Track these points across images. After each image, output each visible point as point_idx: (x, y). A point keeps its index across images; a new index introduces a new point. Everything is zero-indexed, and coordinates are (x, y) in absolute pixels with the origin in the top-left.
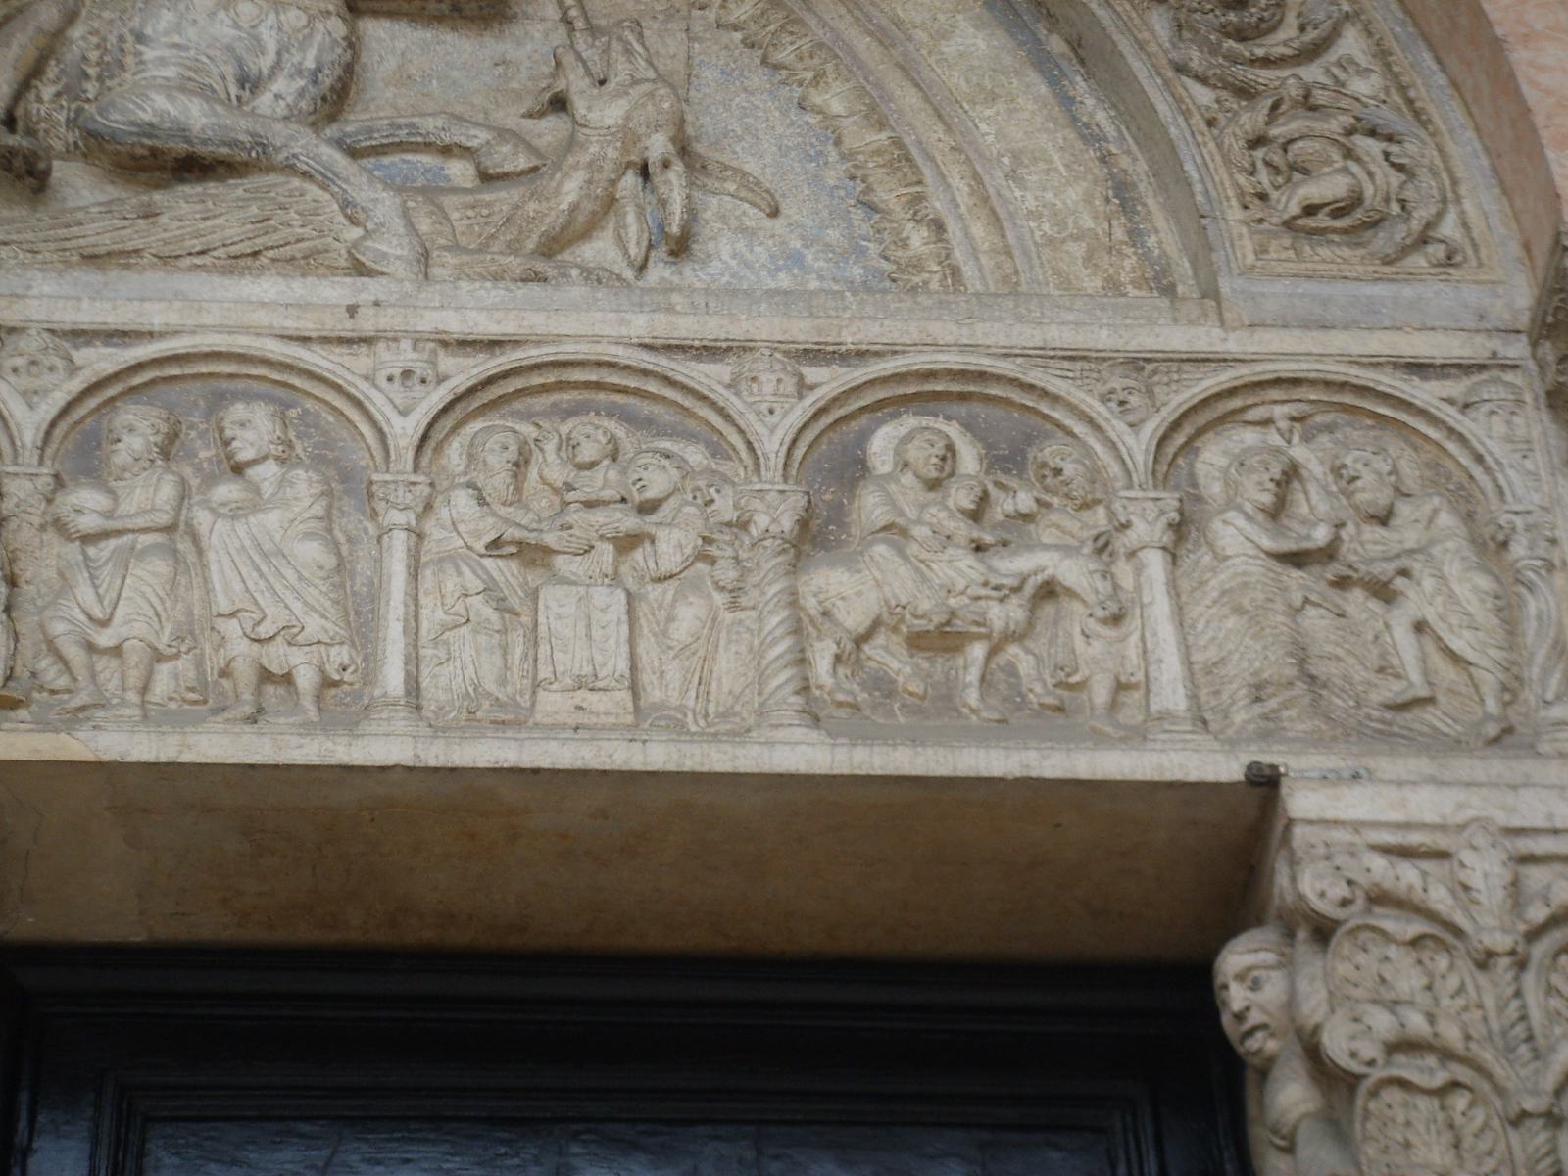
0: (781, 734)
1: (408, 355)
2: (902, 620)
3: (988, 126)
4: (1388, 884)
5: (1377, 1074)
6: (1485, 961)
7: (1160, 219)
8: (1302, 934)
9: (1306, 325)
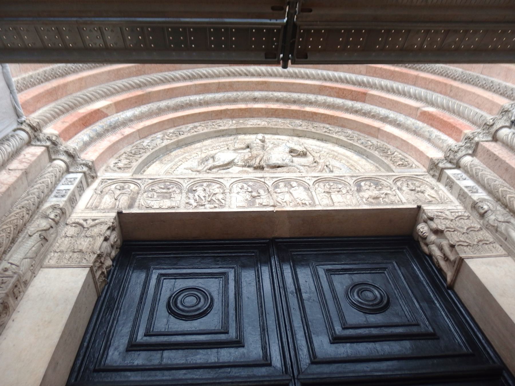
1: (309, 178)
3: (360, 163)
6: (452, 220)
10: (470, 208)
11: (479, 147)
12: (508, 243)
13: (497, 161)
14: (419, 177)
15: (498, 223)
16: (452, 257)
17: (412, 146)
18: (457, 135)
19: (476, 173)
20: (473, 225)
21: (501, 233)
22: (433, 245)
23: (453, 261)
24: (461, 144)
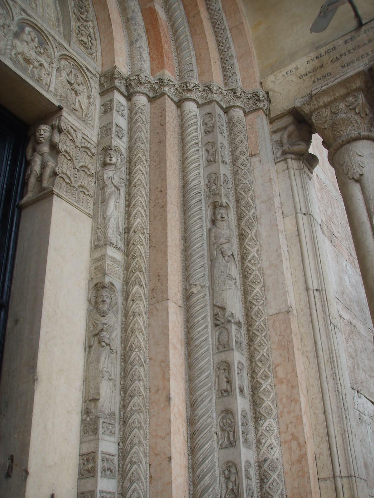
0: (7, 59)
2: (24, 55)
4: (70, 130)
5: (63, 153)
6: (76, 147)
7: (61, 27)
8: (56, 130)
9: (78, 54)
10: (102, 148)
11: (162, 99)
12: (101, 207)
13: (161, 127)
14: (88, 73)
15: (111, 183)
16: (45, 184)
17: (112, 33)
18: (157, 67)
19: (136, 120)
20: (89, 166)
21: (104, 193)
22: (39, 156)
23: (44, 187)
24: (151, 79)
